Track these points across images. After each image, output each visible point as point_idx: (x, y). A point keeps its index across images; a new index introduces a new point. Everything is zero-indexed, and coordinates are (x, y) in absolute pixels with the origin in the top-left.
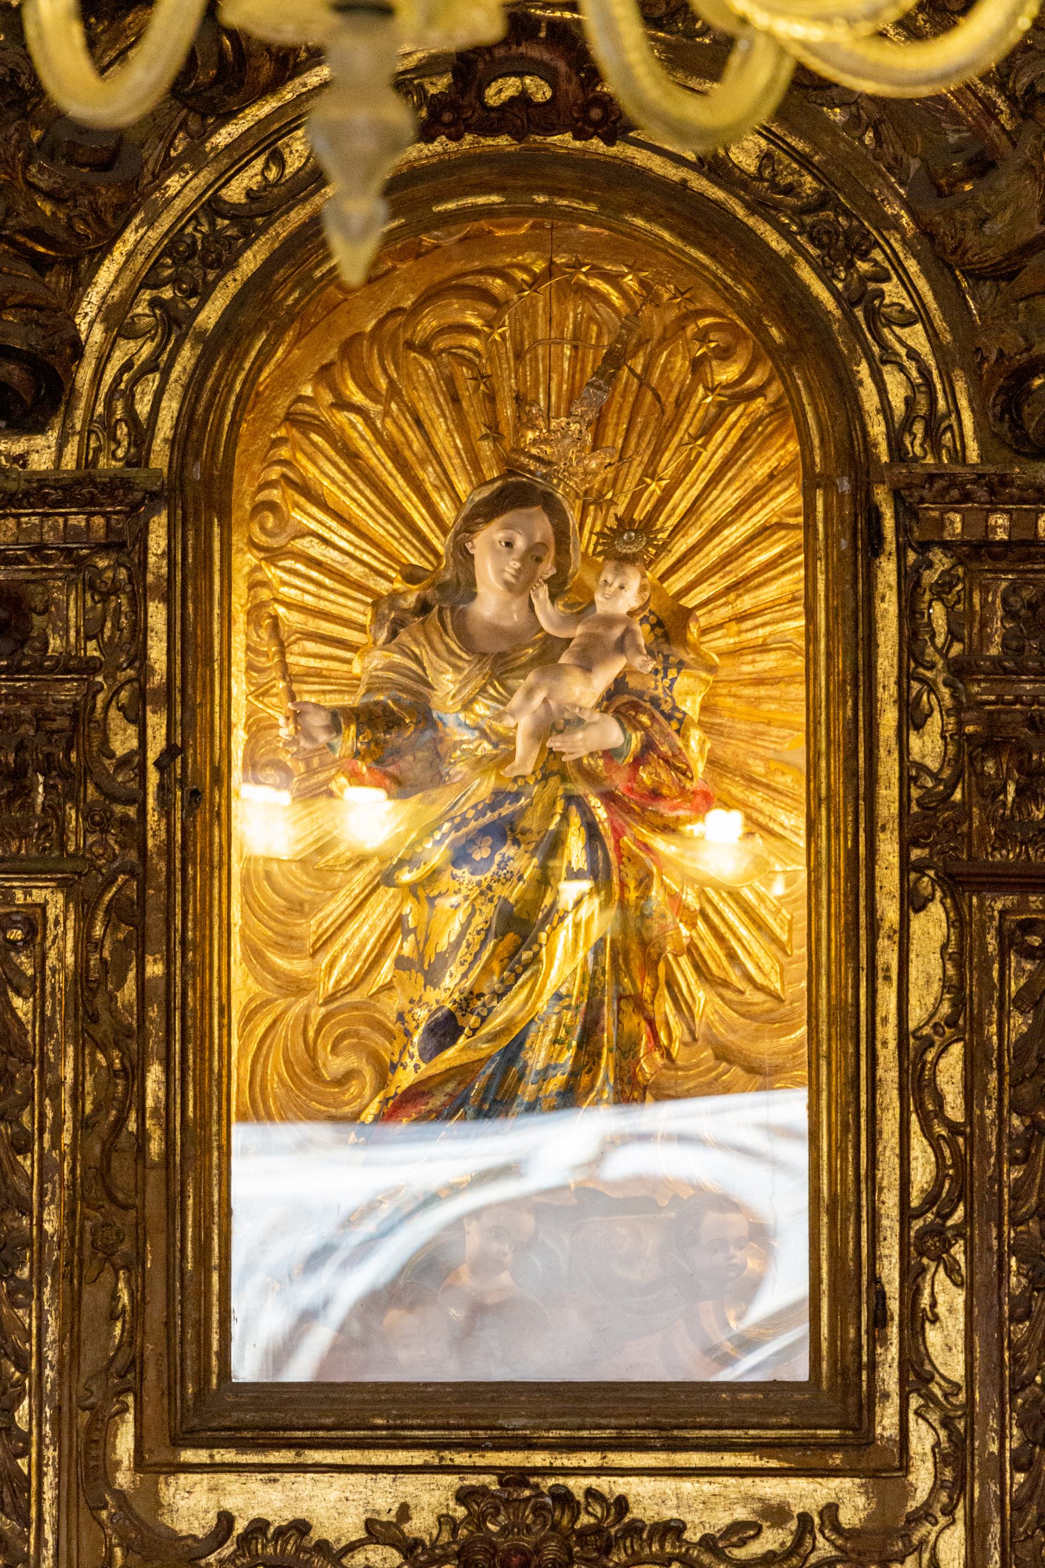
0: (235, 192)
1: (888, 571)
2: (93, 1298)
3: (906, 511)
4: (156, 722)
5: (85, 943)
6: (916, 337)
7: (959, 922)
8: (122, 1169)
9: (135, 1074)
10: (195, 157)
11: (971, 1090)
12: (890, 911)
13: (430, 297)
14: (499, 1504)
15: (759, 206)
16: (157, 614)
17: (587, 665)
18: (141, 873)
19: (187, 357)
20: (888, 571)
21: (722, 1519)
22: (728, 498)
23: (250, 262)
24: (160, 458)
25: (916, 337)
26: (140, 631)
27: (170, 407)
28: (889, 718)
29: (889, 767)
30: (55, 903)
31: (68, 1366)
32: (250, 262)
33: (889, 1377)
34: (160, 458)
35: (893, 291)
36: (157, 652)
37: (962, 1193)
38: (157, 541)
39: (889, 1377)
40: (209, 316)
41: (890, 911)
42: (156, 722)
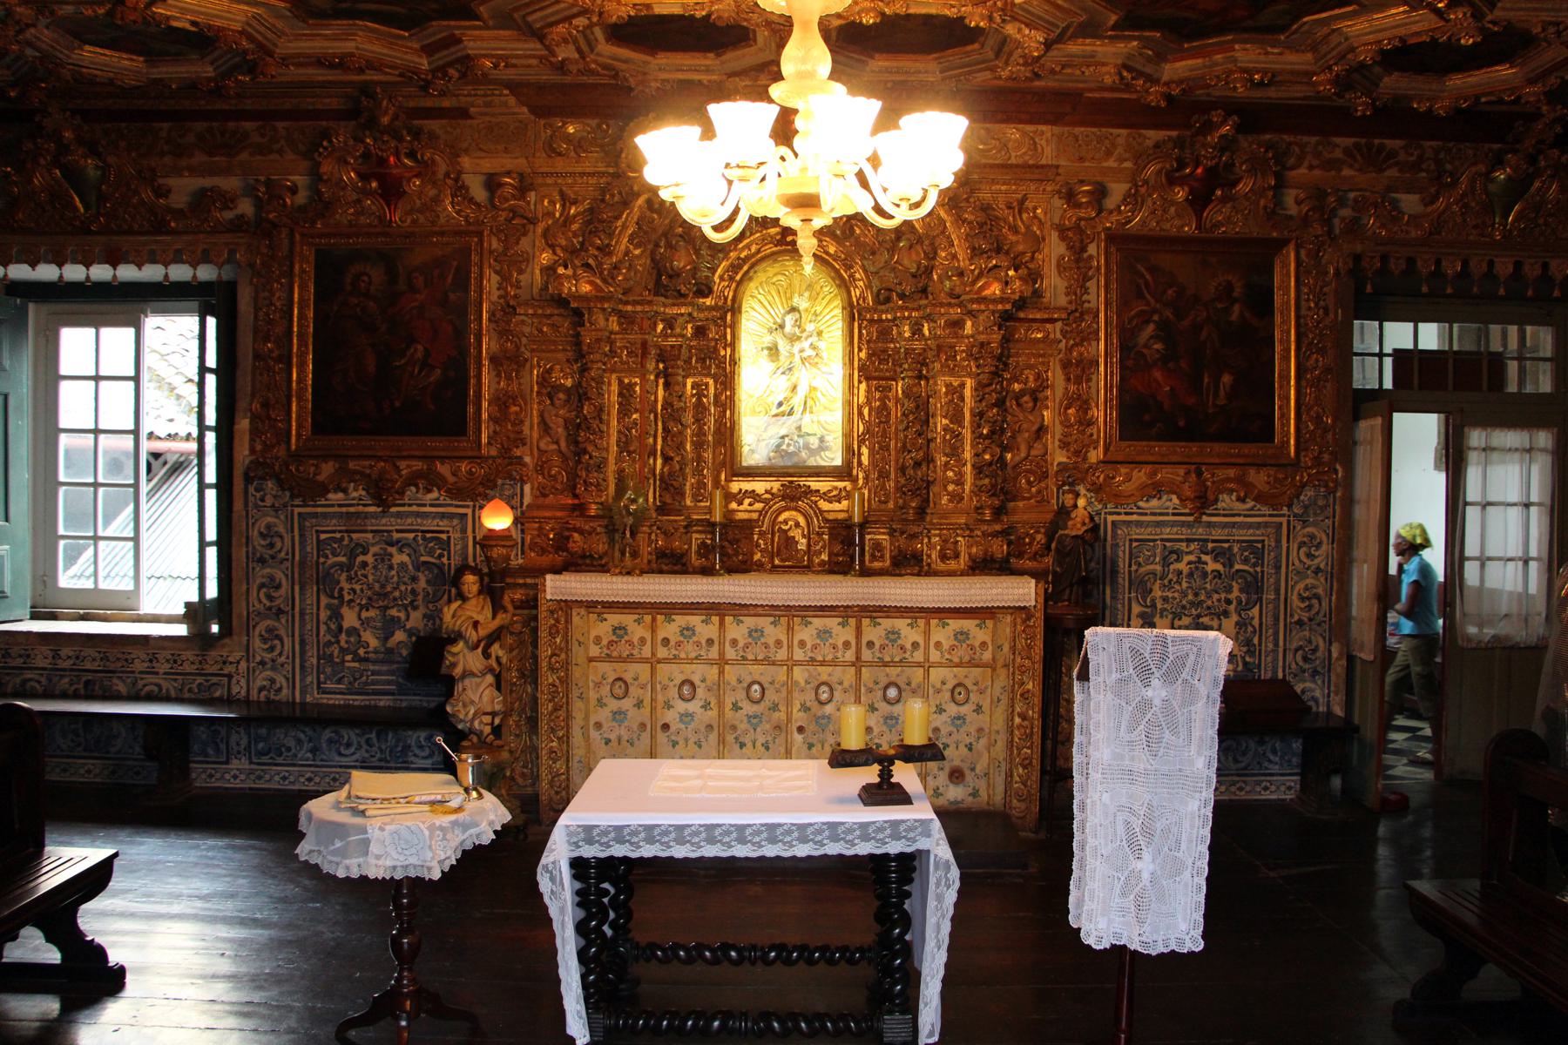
0: (742, 256)
1: (856, 324)
2: (717, 451)
3: (859, 314)
4: (729, 350)
5: (716, 389)
6: (861, 283)
7: (868, 386)
8: (723, 430)
9: (725, 412)
10: (735, 249)
11: (870, 415)
12: (856, 384)
13: (775, 275)
14: (788, 487)
15: (835, 260)
16: (729, 330)
17: (806, 338)
18: (726, 376)
19: (734, 285)
20: (856, 324)
21: (826, 489)
22: (827, 310)
23: (745, 268)
24: (729, 302)
25: (861, 283)
26: (725, 334)
27: (731, 294)
28: (856, 350)
29: (856, 359)
30: (711, 382)
31: (713, 463)
32: (745, 268)
33: (855, 464)
34: (729, 302)
35: (857, 276)
36: (729, 337)
37: (868, 432)
38: (729, 317)
39: (855, 464)
40: (738, 278)
41: (856, 384)
42: (729, 350)
